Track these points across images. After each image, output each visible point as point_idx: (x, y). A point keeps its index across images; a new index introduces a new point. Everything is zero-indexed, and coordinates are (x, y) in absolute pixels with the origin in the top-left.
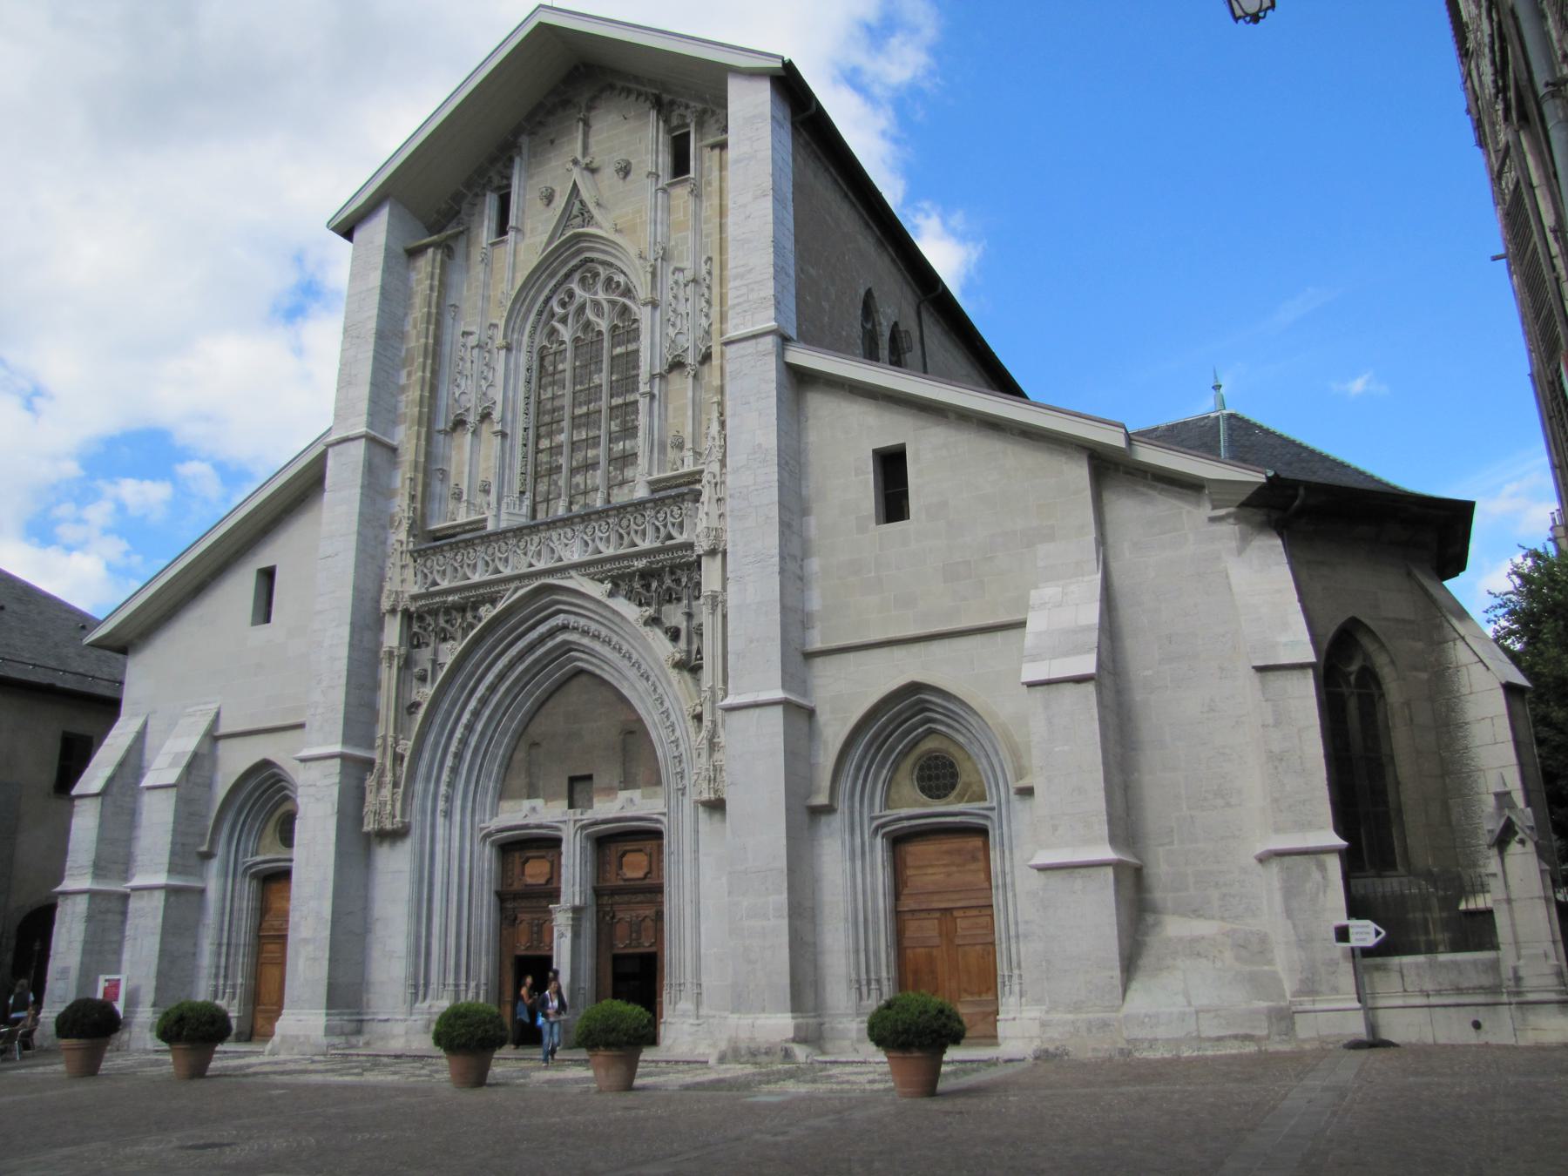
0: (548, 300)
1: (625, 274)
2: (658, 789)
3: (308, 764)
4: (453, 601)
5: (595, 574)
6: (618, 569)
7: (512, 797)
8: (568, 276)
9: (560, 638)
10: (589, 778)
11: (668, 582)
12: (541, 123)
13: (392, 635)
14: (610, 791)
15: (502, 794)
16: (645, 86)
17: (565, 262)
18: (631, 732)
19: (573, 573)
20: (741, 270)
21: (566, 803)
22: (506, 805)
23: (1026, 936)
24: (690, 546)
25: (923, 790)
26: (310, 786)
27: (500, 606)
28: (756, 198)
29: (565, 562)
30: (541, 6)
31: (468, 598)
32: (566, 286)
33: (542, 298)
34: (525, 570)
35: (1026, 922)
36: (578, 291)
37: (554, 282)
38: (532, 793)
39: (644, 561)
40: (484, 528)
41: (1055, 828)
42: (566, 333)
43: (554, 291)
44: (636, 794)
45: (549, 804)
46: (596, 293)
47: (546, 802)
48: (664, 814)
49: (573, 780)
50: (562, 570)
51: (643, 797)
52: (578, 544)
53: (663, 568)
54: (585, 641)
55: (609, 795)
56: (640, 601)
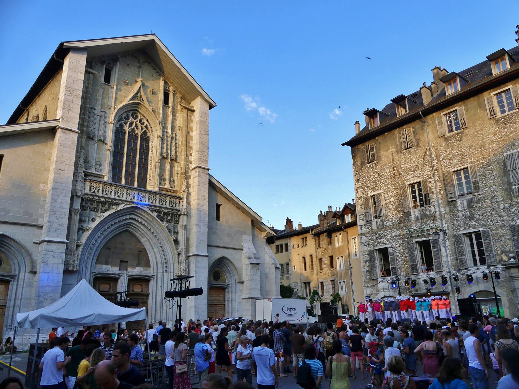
0: (122, 114)
1: (147, 121)
2: (149, 268)
3: (49, 243)
4: (104, 201)
5: (151, 208)
6: (158, 210)
7: (100, 264)
8: (130, 111)
9: (128, 221)
10: (127, 262)
11: (169, 218)
12: (125, 56)
13: (77, 205)
14: (133, 267)
15: (97, 262)
16: (161, 72)
17: (132, 107)
18: (140, 251)
19: (145, 206)
20: (202, 150)
21: (119, 268)
22: (98, 266)
23: (237, 311)
24: (179, 211)
25: (214, 279)
26: (50, 251)
27: (120, 208)
28: (205, 134)
29: (142, 202)
30: (154, 34)
31: (108, 201)
32: (127, 113)
33: (121, 113)
34: (129, 200)
35: (238, 308)
36: (131, 118)
37: (126, 110)
38: (107, 263)
39: (167, 211)
40: (103, 178)
41: (253, 291)
42: (127, 129)
43: (124, 112)
44: (142, 269)
45: (113, 267)
46: (137, 121)
47: (112, 267)
48: (154, 276)
49: (121, 261)
50: (143, 205)
51: (144, 270)
52: (147, 199)
53: (170, 213)
54: (137, 224)
55: (133, 268)
56: (161, 220)
